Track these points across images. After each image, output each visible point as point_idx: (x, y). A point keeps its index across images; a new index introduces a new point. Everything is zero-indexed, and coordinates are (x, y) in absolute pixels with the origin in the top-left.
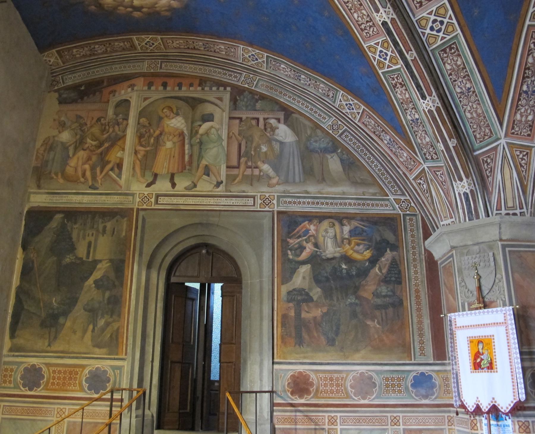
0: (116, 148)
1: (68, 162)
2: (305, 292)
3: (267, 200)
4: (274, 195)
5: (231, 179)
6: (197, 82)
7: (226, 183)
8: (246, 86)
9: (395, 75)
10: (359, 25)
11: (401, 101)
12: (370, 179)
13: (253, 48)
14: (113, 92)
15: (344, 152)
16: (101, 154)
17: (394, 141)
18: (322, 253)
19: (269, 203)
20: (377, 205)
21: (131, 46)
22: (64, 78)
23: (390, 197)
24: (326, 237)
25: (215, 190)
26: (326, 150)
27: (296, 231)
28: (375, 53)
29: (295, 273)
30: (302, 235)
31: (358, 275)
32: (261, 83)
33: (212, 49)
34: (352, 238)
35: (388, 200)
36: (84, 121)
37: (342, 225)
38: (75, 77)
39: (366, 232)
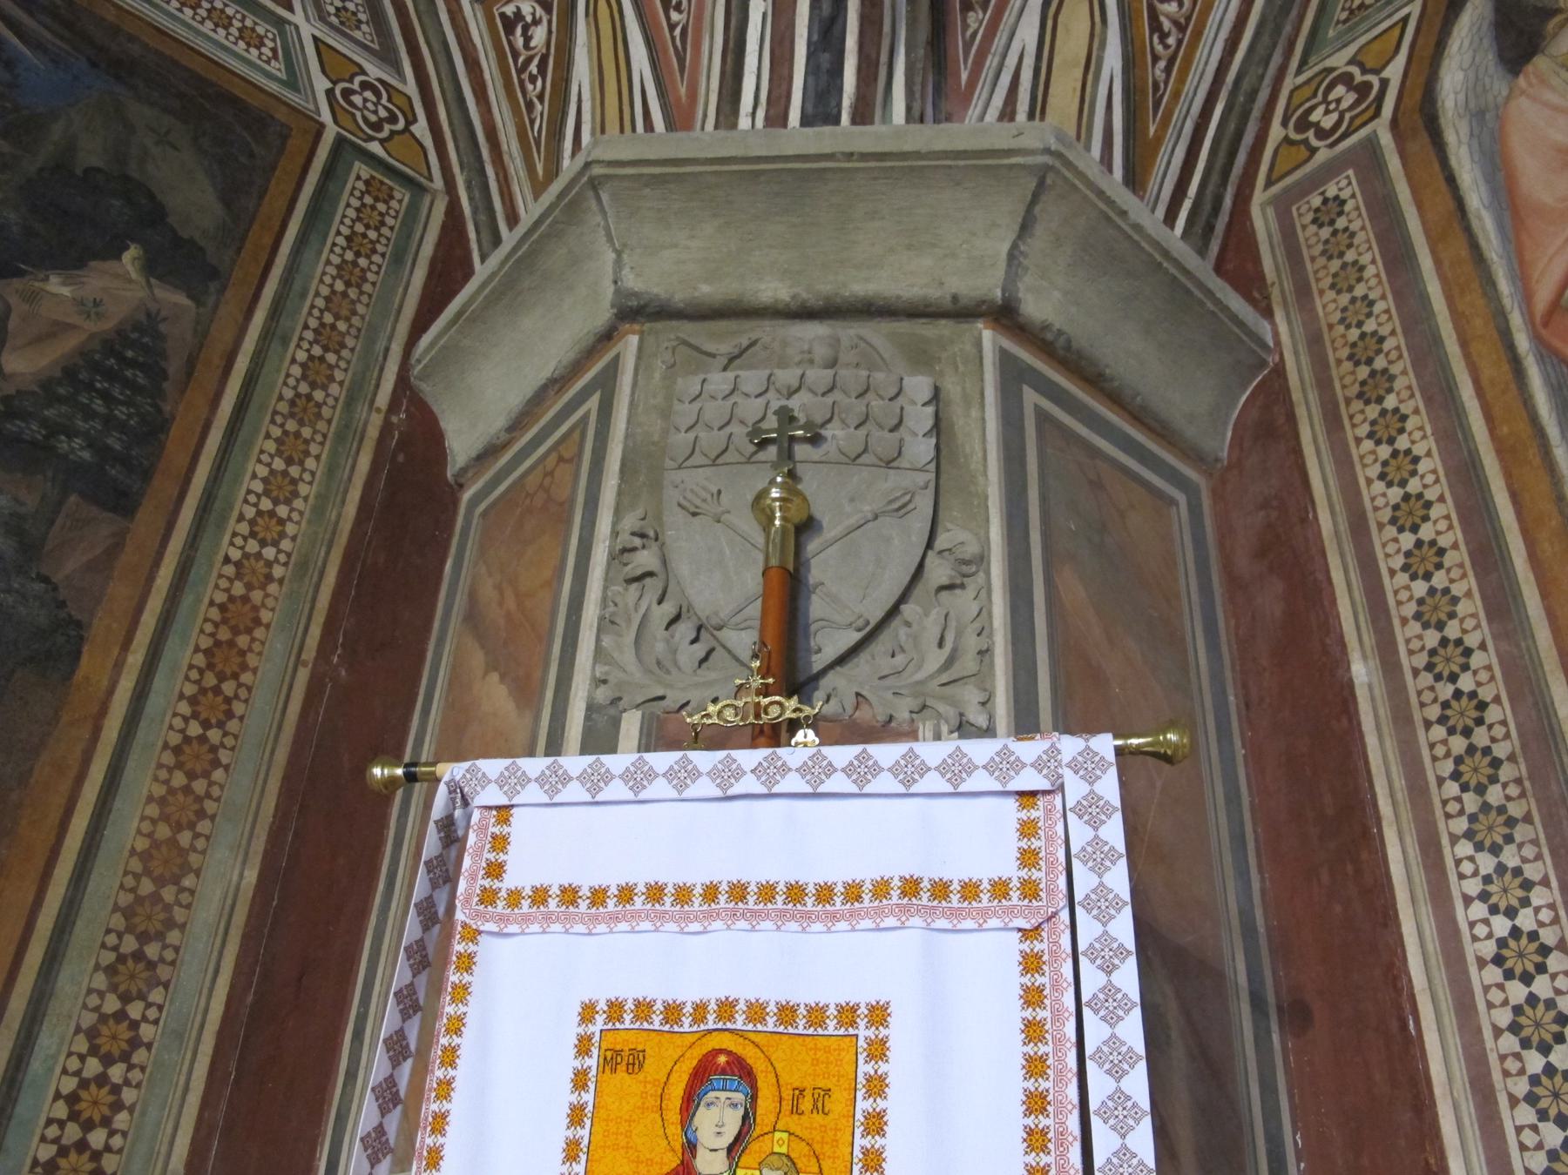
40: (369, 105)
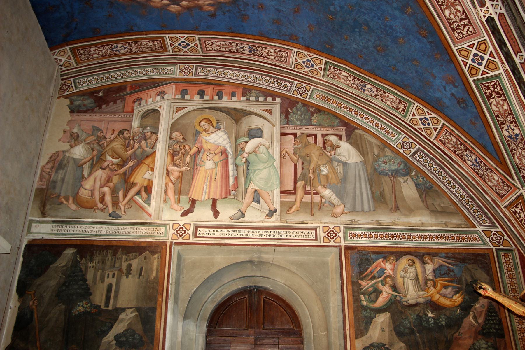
0: (144, 168)
1: (82, 183)
2: (385, 348)
3: (332, 232)
4: (340, 227)
5: (287, 207)
6: (240, 90)
7: (281, 212)
8: (299, 96)
9: (490, 83)
10: (450, 24)
11: (496, 113)
12: (453, 207)
13: (310, 52)
14: (139, 100)
15: (419, 175)
16: (124, 174)
17: (481, 162)
18: (402, 298)
19: (334, 237)
20: (463, 238)
21: (162, 47)
22: (77, 81)
23: (478, 229)
24: (406, 278)
25: (266, 220)
26: (397, 173)
27: (369, 270)
28: (467, 57)
29: (371, 323)
30: (377, 275)
31: (449, 326)
32: (315, 93)
33: (259, 53)
34: (438, 279)
35: (476, 232)
36: (102, 134)
37: (424, 263)
38: (90, 81)
39: (453, 271)
40: (496, 238)
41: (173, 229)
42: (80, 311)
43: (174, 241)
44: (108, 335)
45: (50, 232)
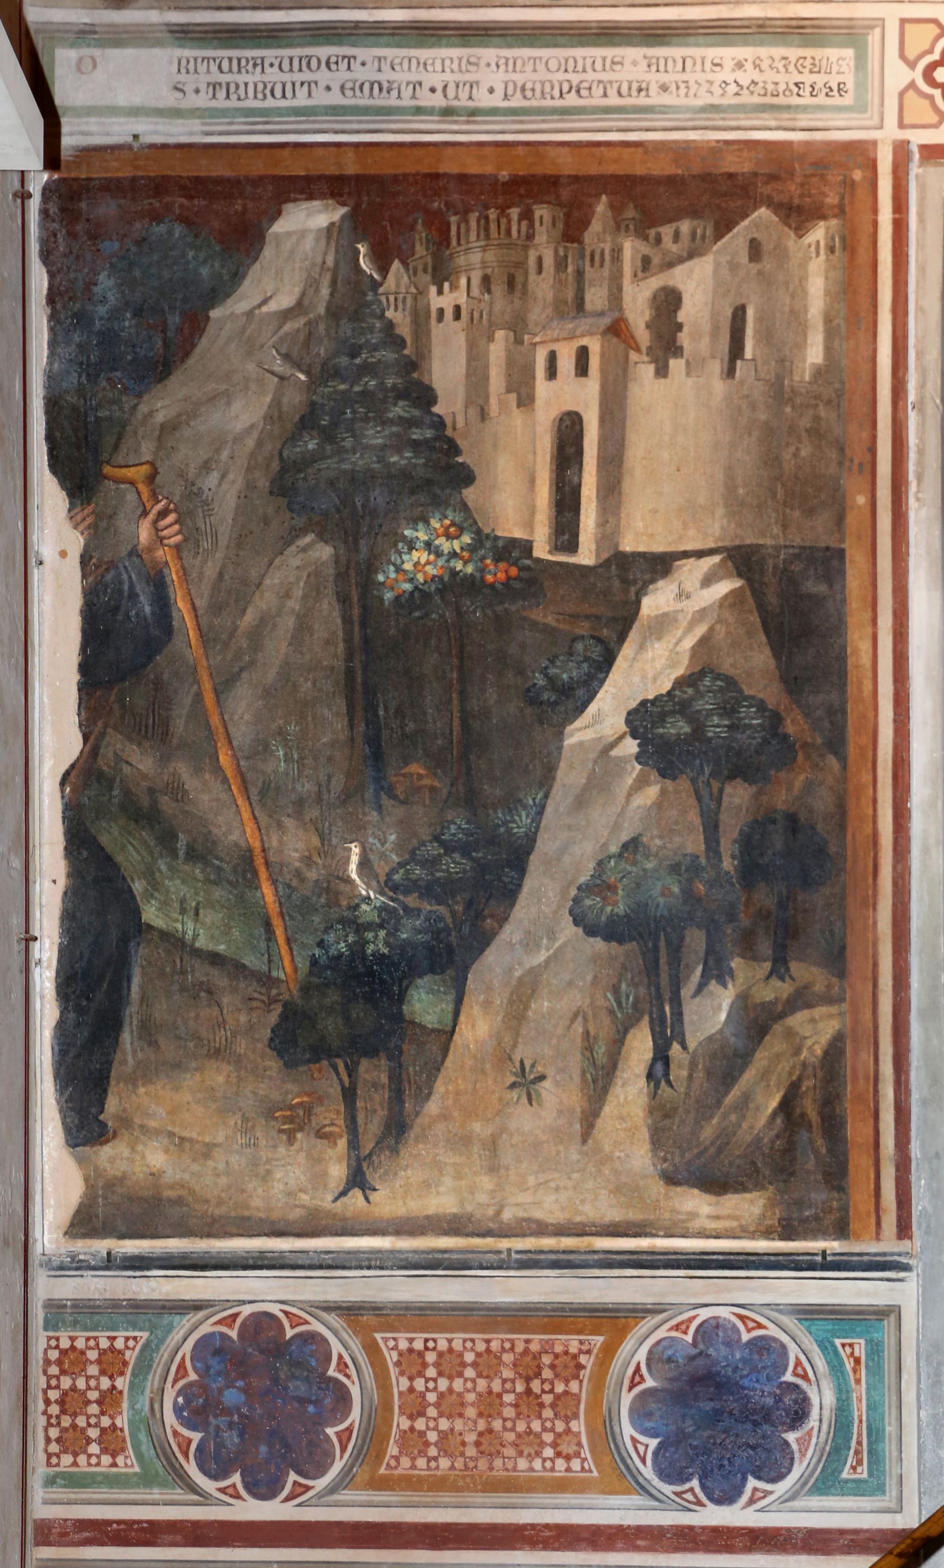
41: (902, 56)
42: (420, 577)
43: (918, 138)
44: (592, 709)
45: (170, 99)
